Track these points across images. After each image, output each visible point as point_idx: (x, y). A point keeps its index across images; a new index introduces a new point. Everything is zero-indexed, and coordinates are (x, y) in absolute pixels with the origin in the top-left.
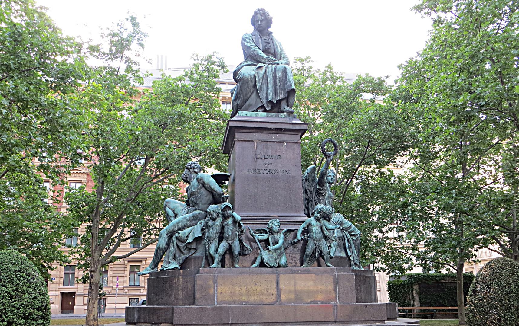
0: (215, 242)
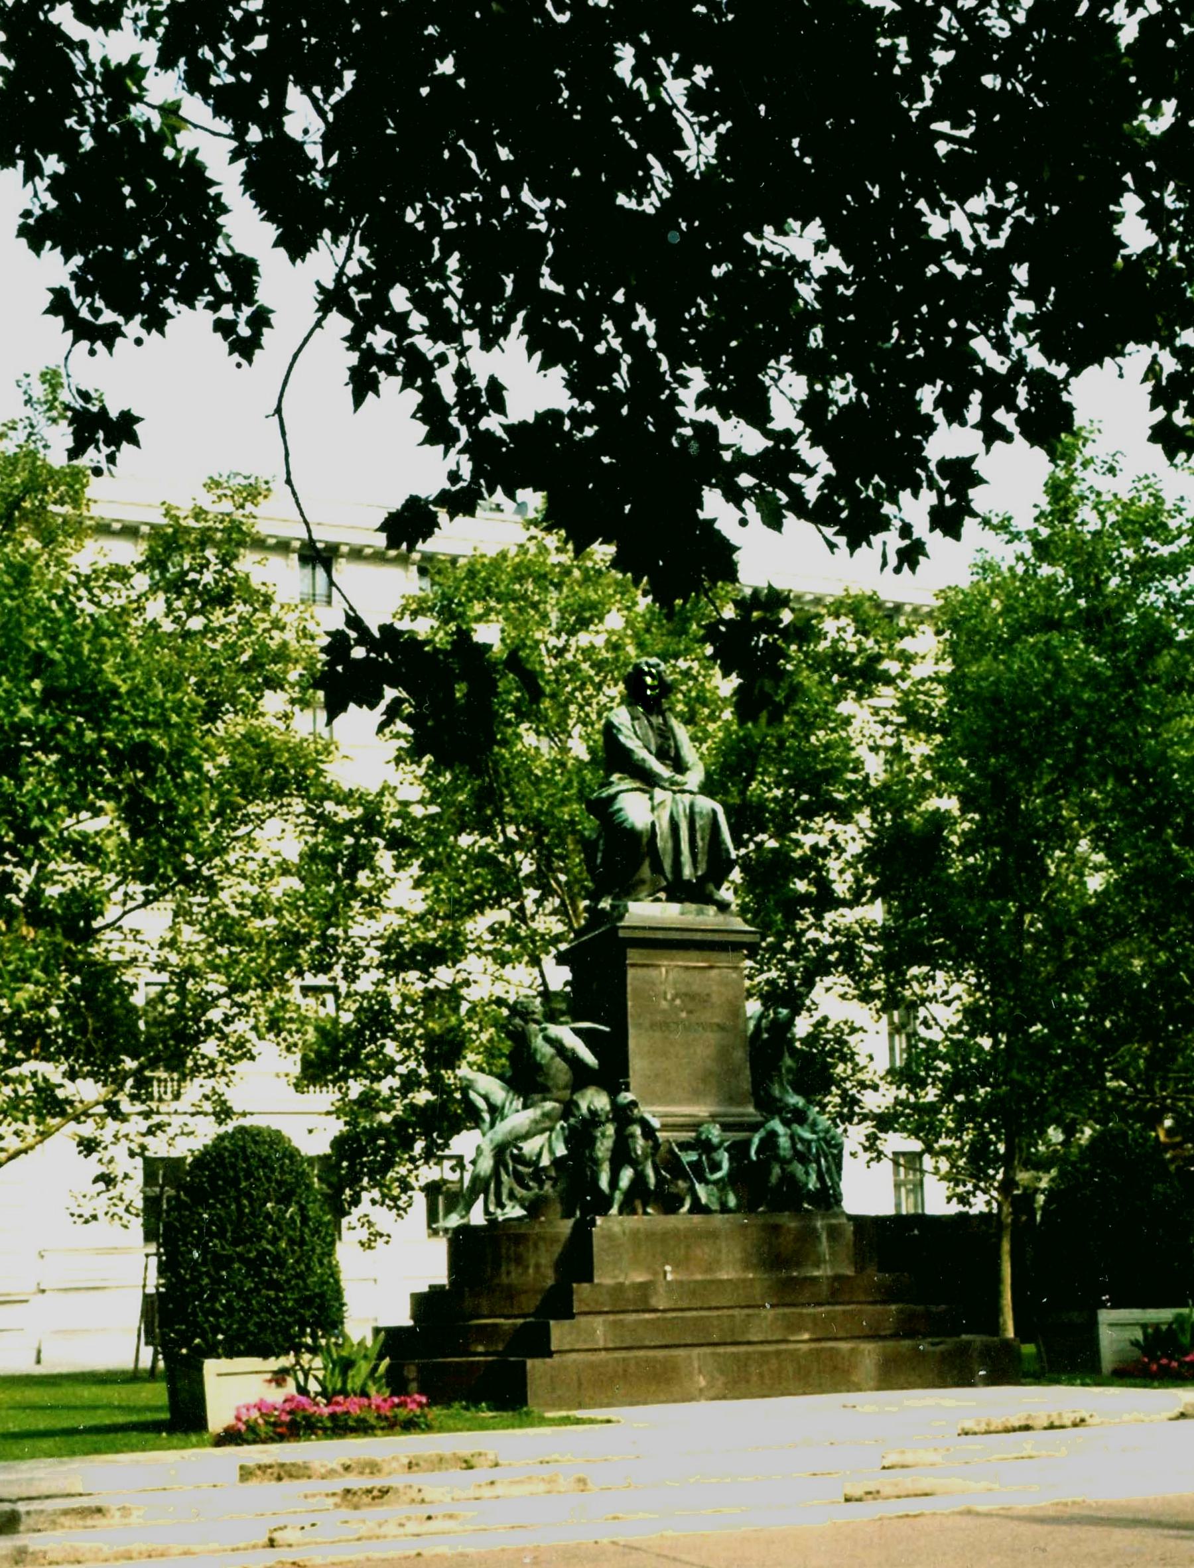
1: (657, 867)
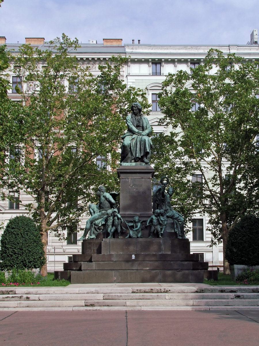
0: (111, 226)
1: (132, 154)
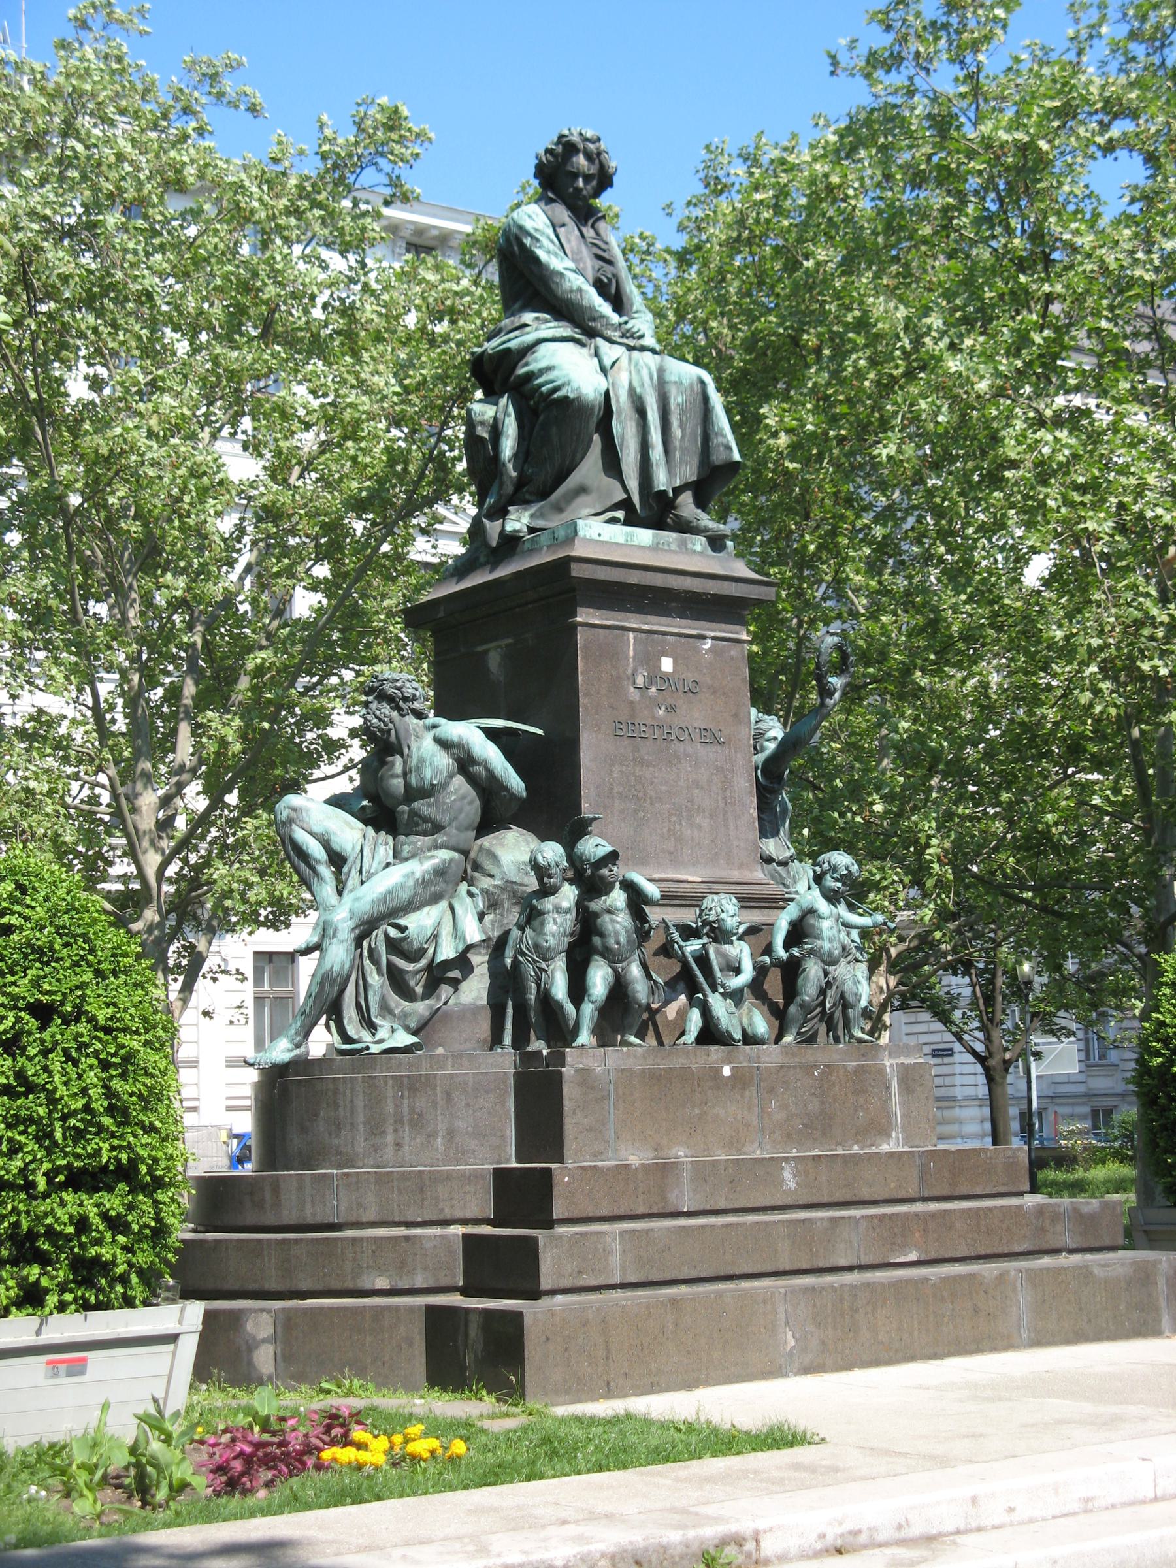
1: (612, 463)
